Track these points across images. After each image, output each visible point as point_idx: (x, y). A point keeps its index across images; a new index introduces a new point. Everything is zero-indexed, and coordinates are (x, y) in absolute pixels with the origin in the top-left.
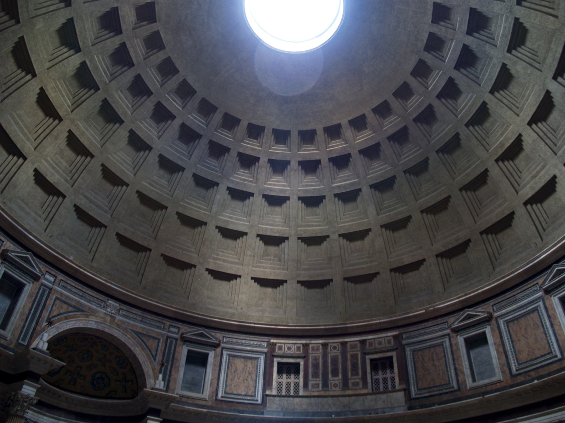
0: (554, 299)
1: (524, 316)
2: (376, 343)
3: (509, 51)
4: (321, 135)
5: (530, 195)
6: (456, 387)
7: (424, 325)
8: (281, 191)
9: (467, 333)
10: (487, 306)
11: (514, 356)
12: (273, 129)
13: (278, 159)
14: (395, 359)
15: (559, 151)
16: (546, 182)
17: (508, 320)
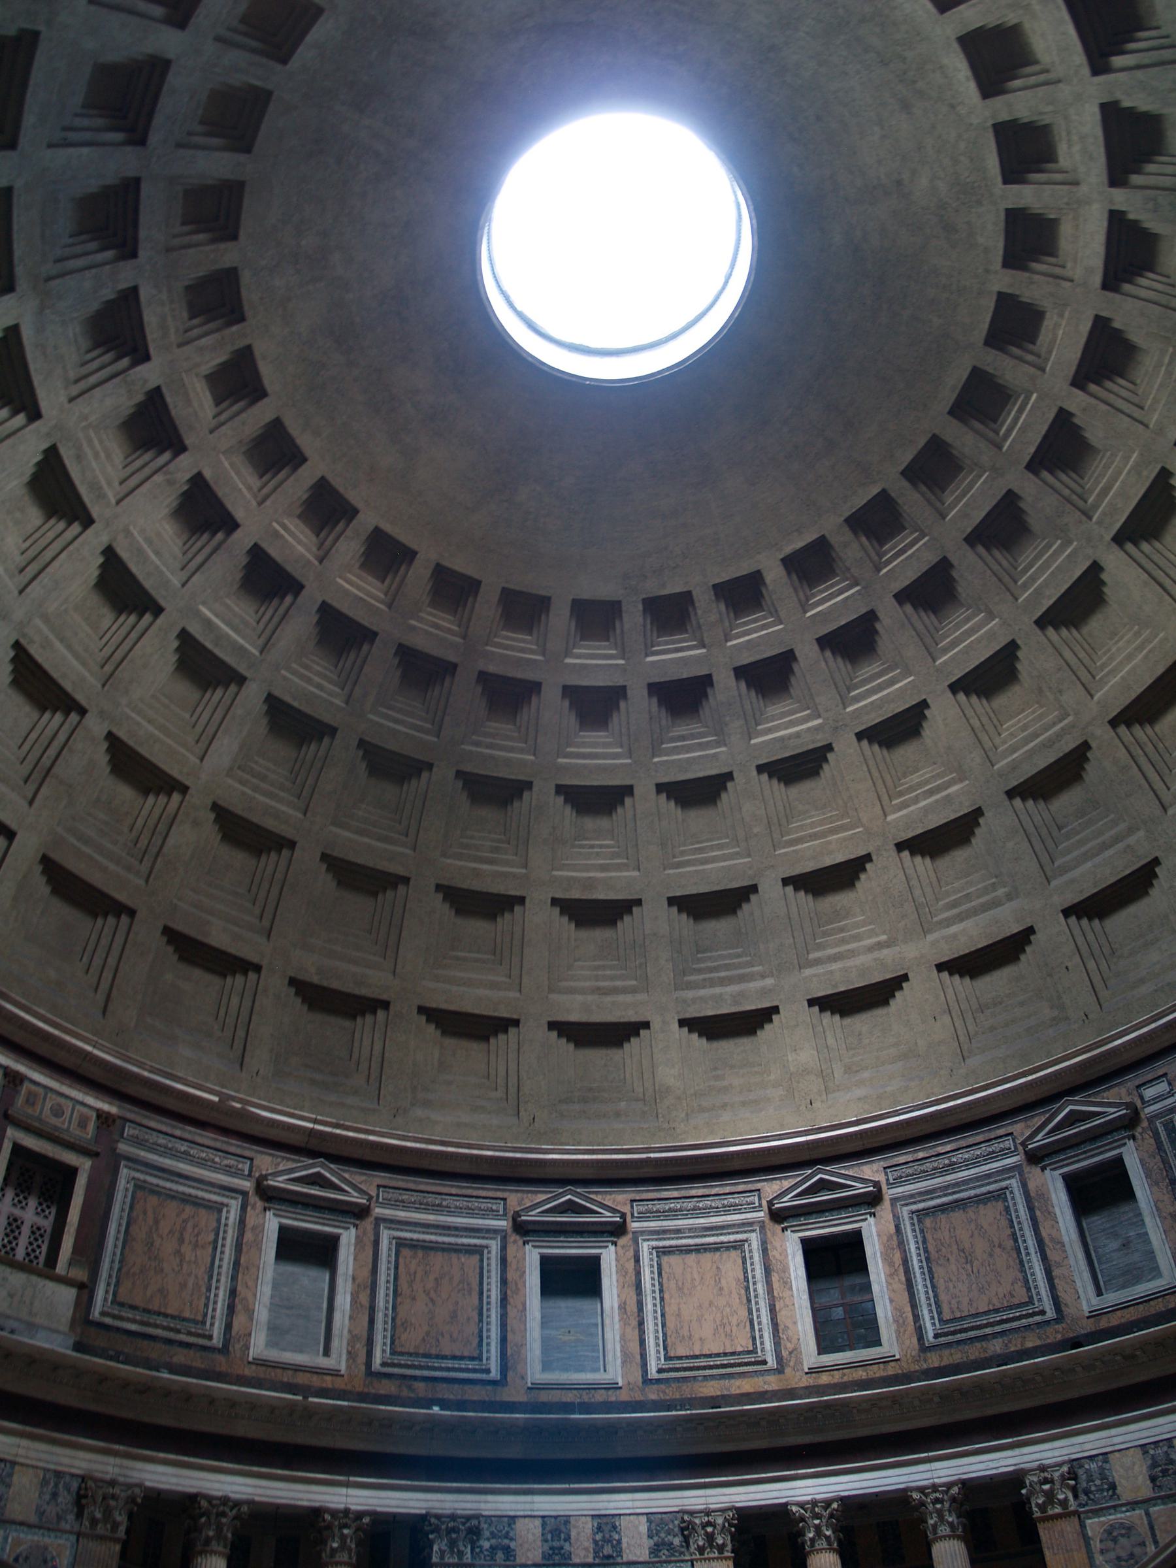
0: (530, 1252)
1: (443, 1250)
2: (48, 1105)
3: (761, 769)
4: (298, 485)
5: (574, 1017)
6: (217, 1340)
7: (190, 1132)
8: (95, 487)
9: (294, 1216)
10: (364, 1178)
11: (389, 1327)
12: (249, 348)
13: (173, 413)
14: (81, 1182)
15: (683, 989)
16: (622, 1020)
17: (405, 1239)
